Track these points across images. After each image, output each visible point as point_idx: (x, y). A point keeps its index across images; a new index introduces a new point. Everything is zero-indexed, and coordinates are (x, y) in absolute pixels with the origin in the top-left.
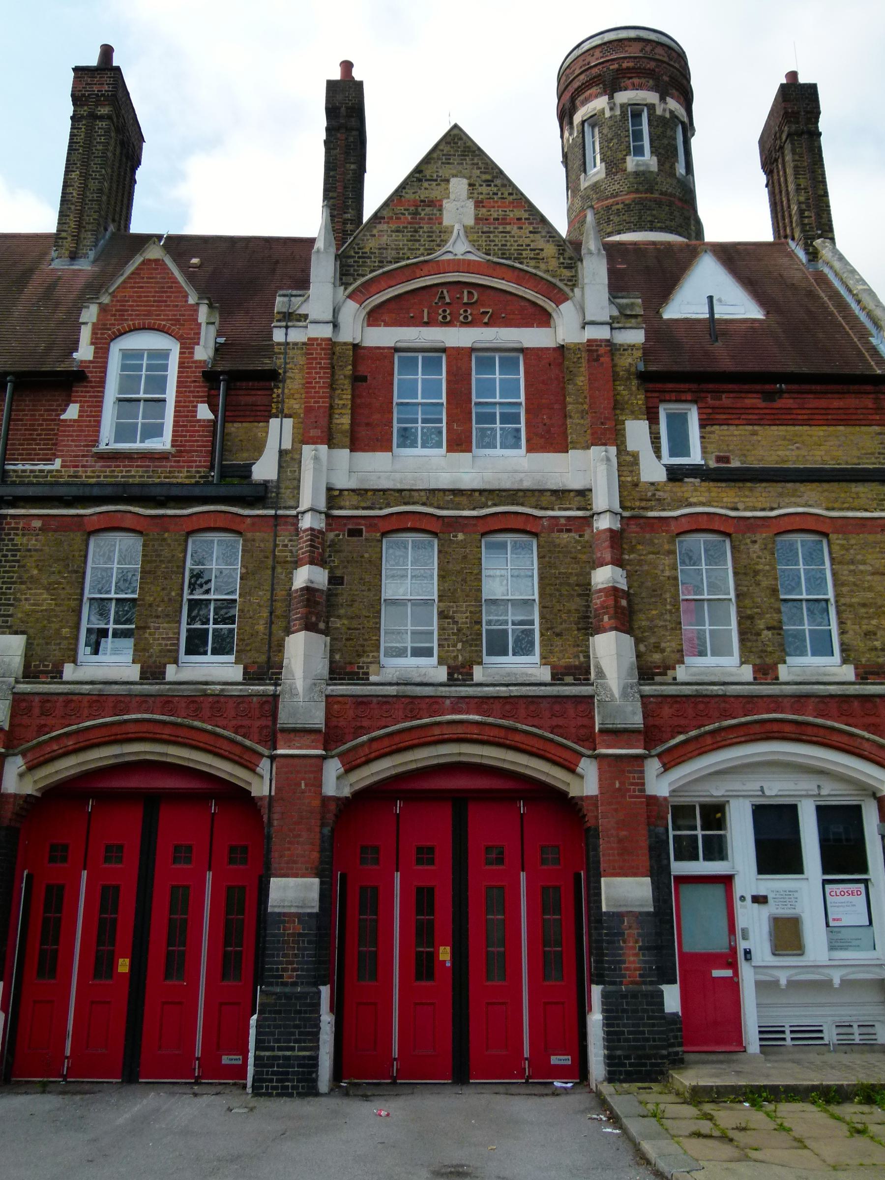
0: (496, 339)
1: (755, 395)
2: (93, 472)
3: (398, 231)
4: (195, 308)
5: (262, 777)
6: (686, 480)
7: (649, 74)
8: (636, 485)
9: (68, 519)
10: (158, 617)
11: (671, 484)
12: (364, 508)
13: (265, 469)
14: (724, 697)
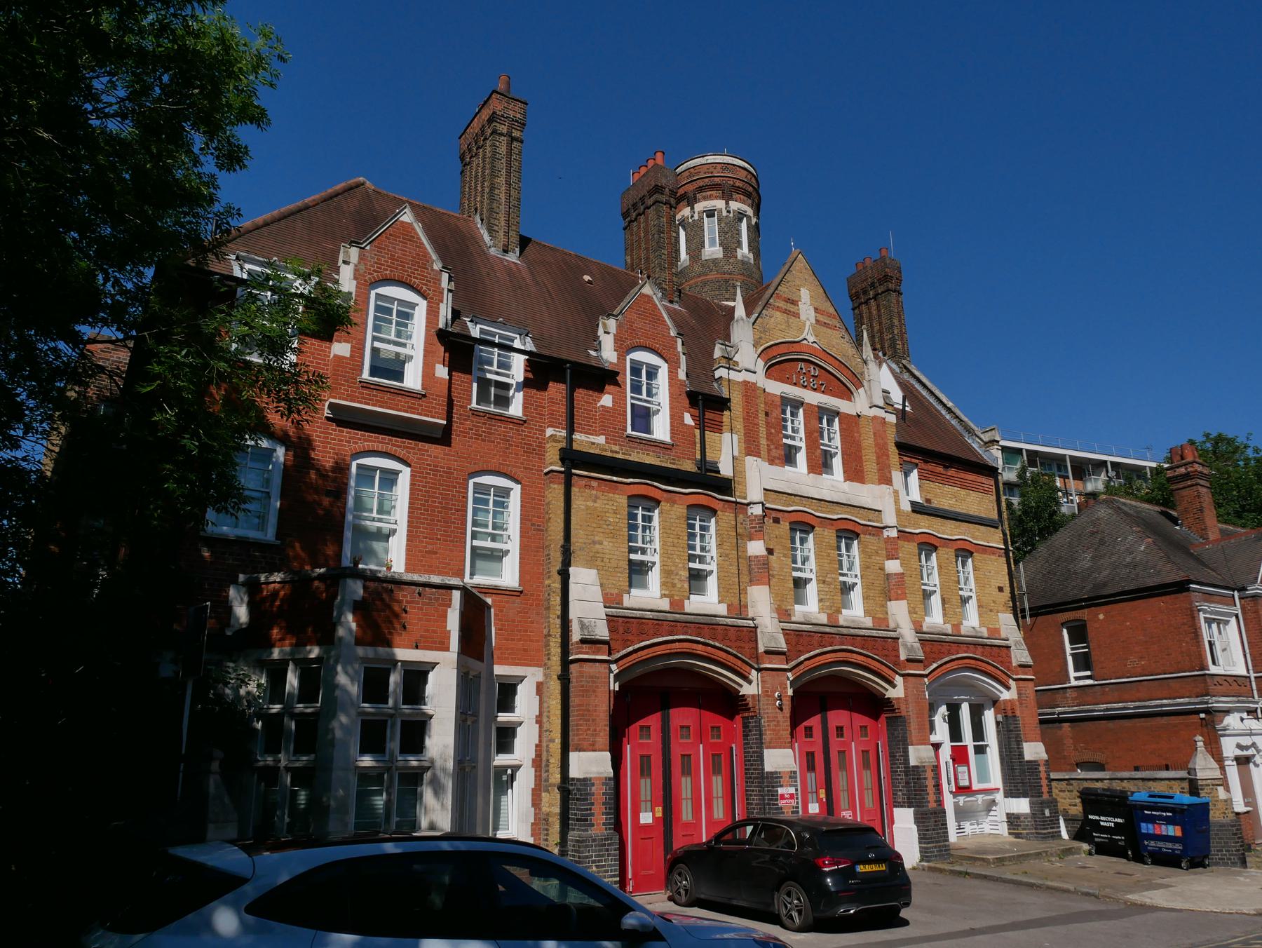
4: (674, 340)
7: (749, 195)
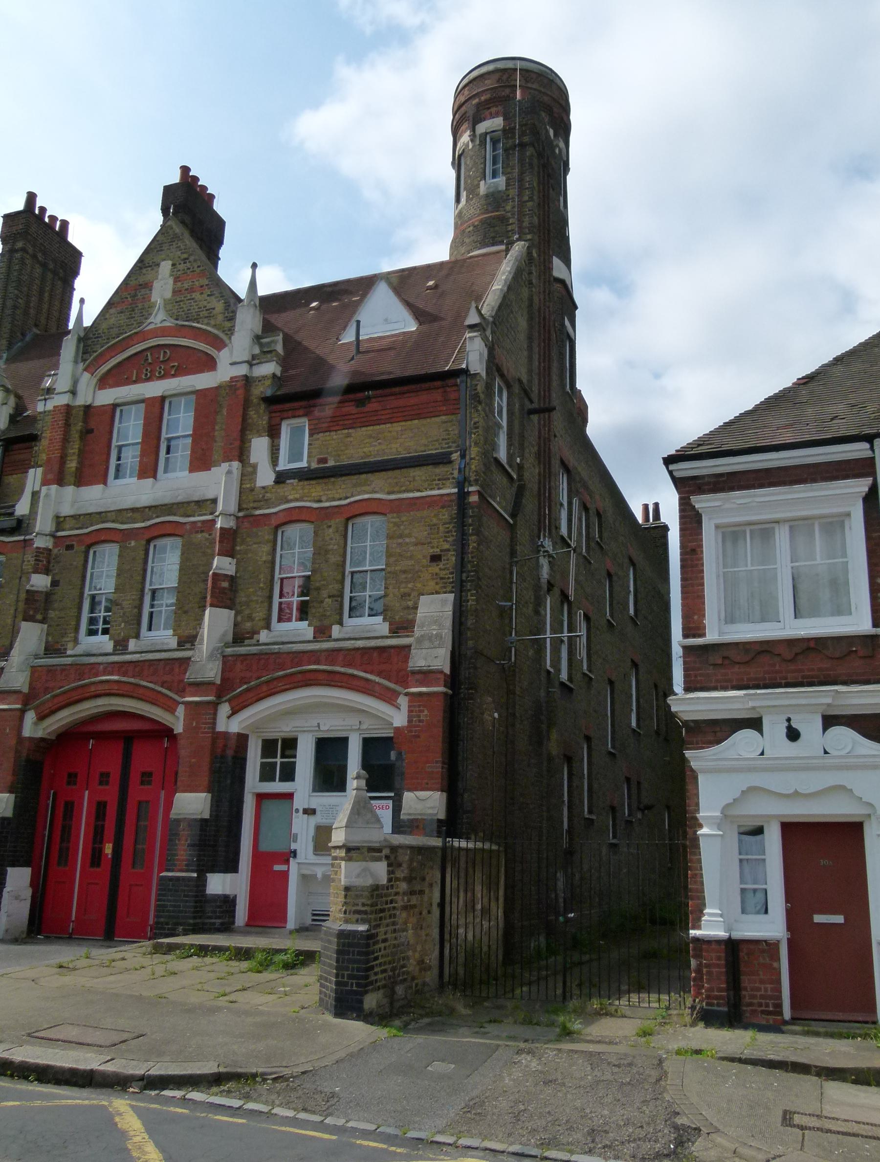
0: (179, 386)
1: (350, 404)
3: (122, 312)
6: (288, 481)
8: (252, 490)
11: (277, 486)
12: (77, 529)
14: (279, 654)
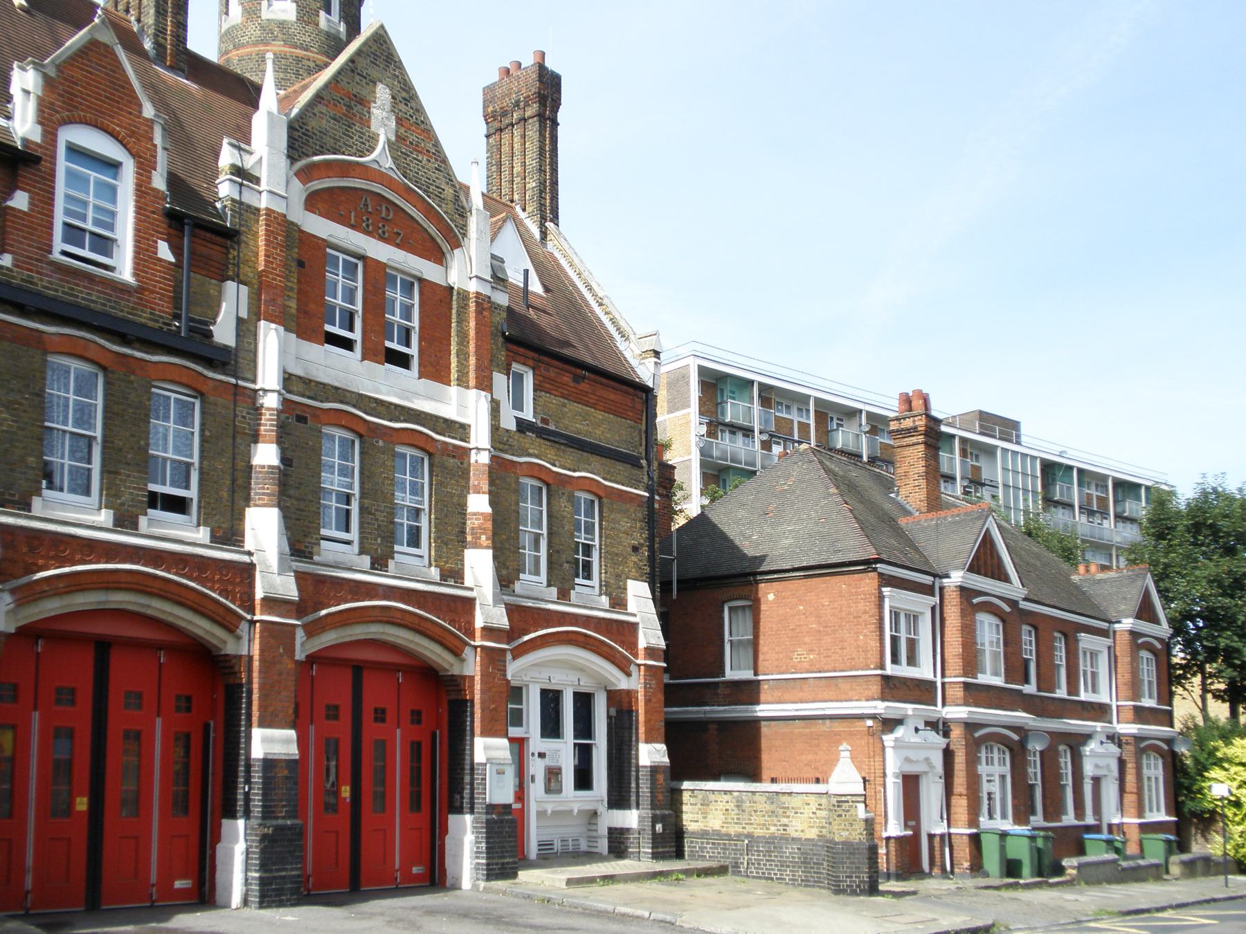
2: (49, 282)
5: (239, 638)
9: (27, 332)
10: (128, 464)
12: (309, 398)
13: (224, 332)
